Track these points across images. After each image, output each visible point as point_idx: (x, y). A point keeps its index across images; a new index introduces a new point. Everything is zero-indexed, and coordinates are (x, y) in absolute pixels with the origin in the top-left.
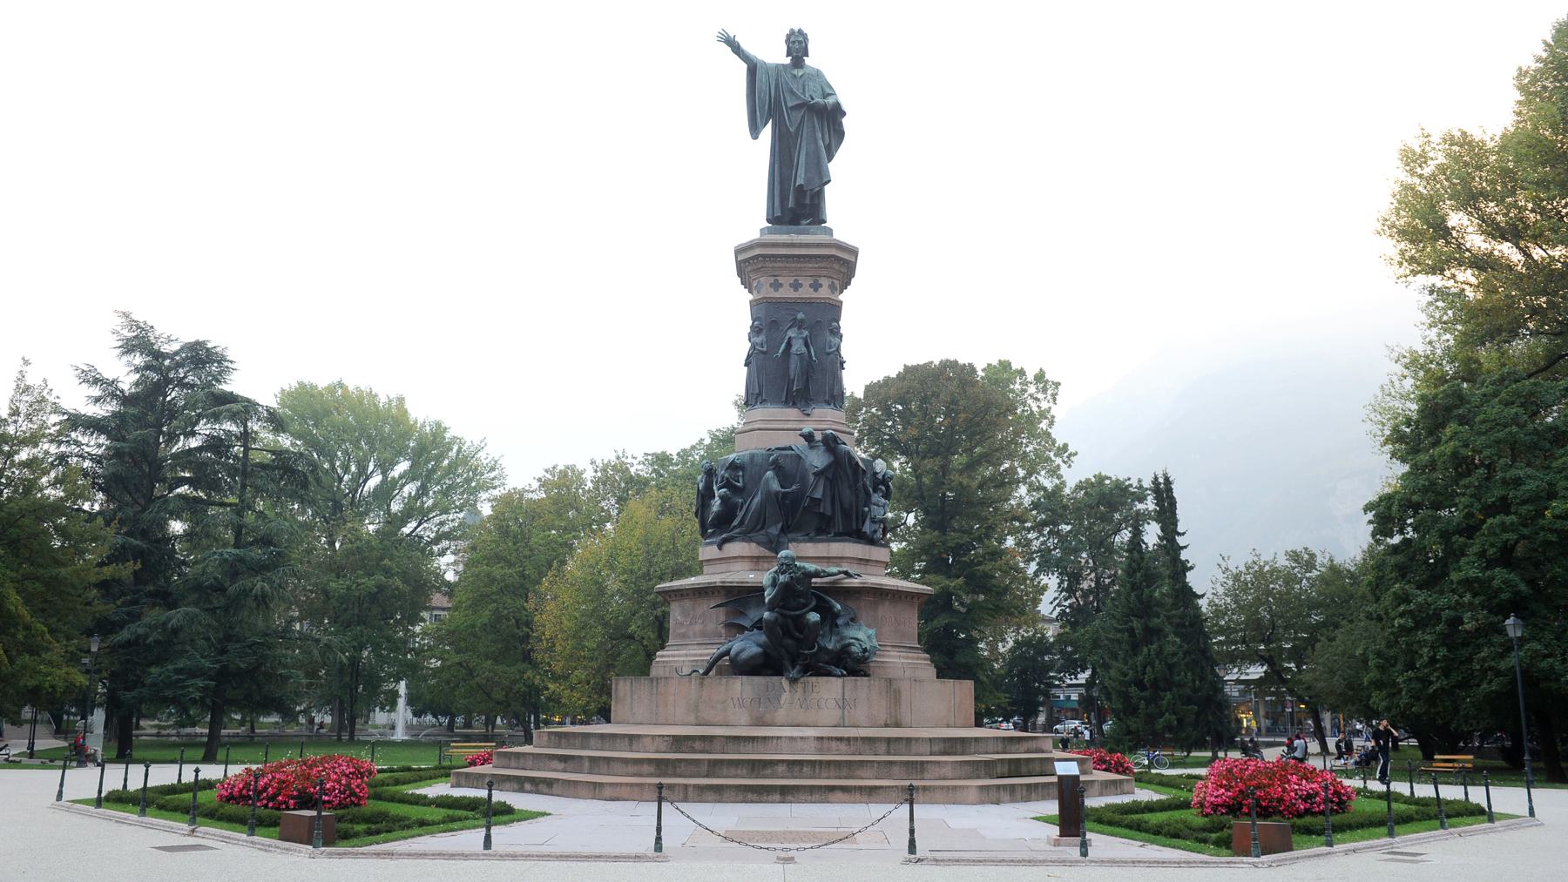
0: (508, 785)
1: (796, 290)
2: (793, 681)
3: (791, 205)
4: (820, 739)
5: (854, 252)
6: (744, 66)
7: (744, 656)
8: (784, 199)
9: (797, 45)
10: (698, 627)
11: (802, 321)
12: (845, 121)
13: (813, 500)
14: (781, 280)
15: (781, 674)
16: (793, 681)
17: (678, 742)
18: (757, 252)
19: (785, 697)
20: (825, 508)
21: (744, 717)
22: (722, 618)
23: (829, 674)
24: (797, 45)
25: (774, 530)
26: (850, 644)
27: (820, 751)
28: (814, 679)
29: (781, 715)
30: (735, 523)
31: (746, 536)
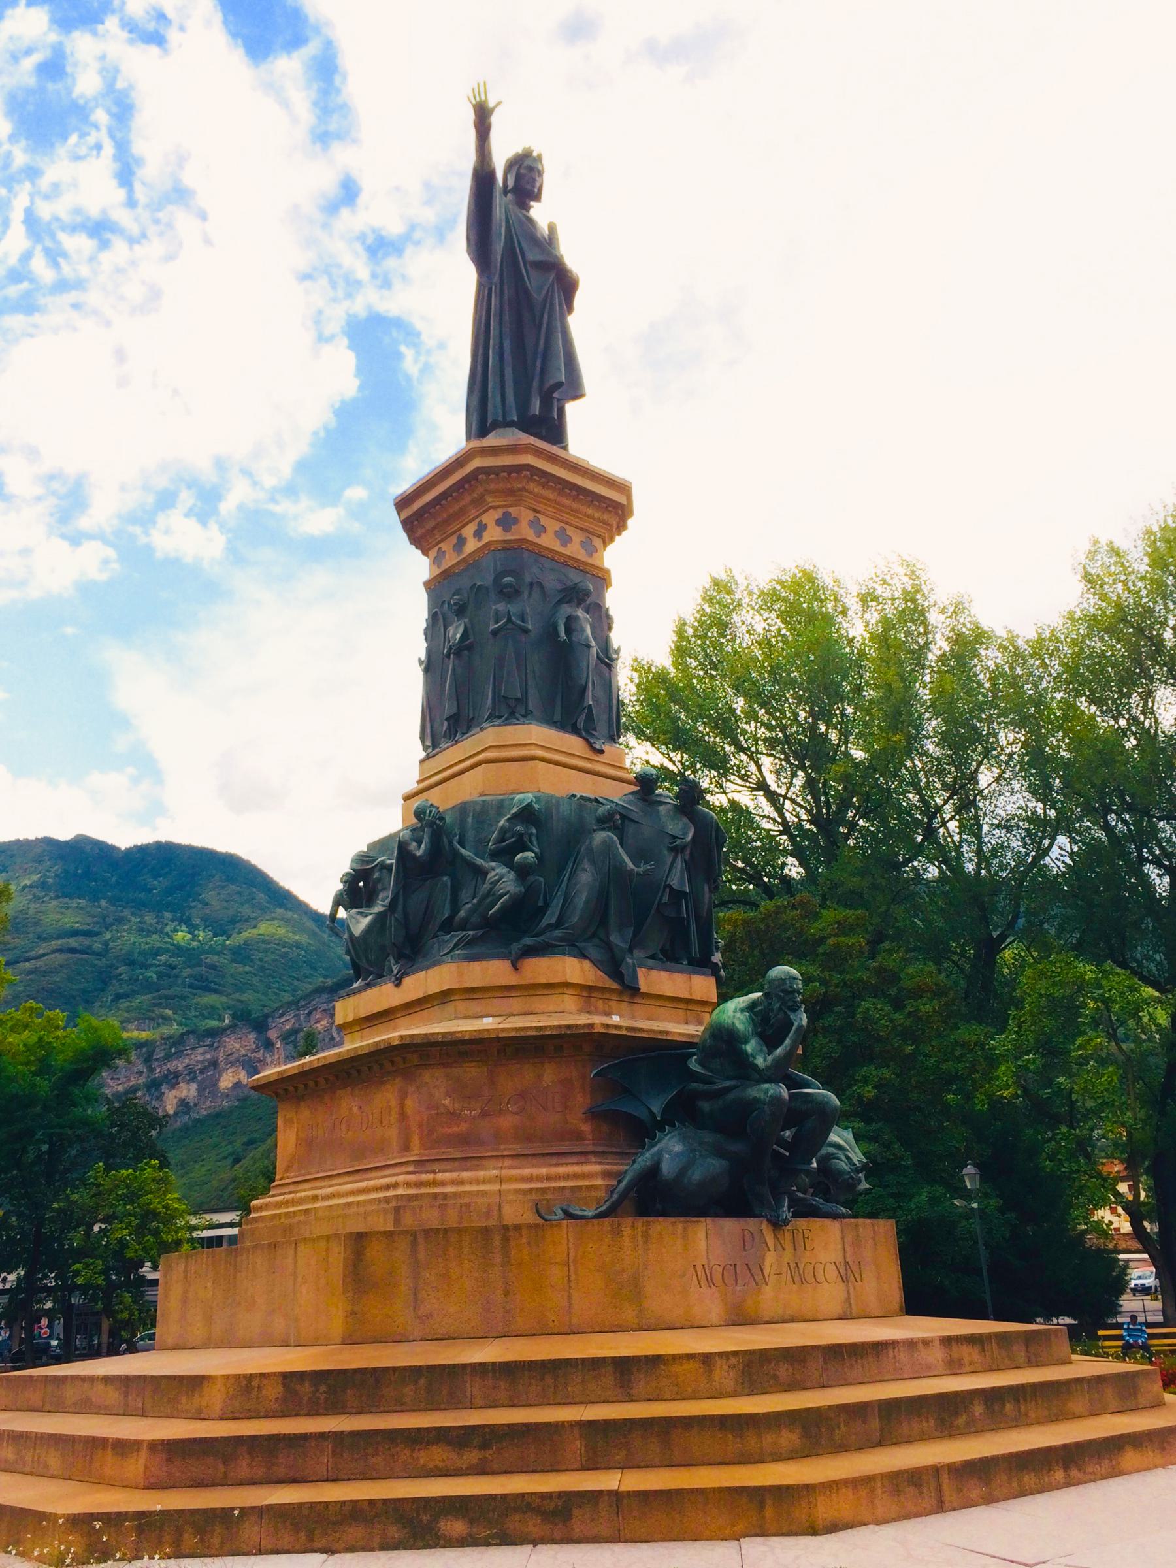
0: (355, 1532)
4: (947, 1341)
10: (507, 1122)
14: (544, 521)
17: (757, 1369)
21: (711, 1305)
22: (581, 1101)
26: (830, 1156)
27: (954, 1367)
29: (769, 1298)
30: (550, 917)
31: (574, 946)
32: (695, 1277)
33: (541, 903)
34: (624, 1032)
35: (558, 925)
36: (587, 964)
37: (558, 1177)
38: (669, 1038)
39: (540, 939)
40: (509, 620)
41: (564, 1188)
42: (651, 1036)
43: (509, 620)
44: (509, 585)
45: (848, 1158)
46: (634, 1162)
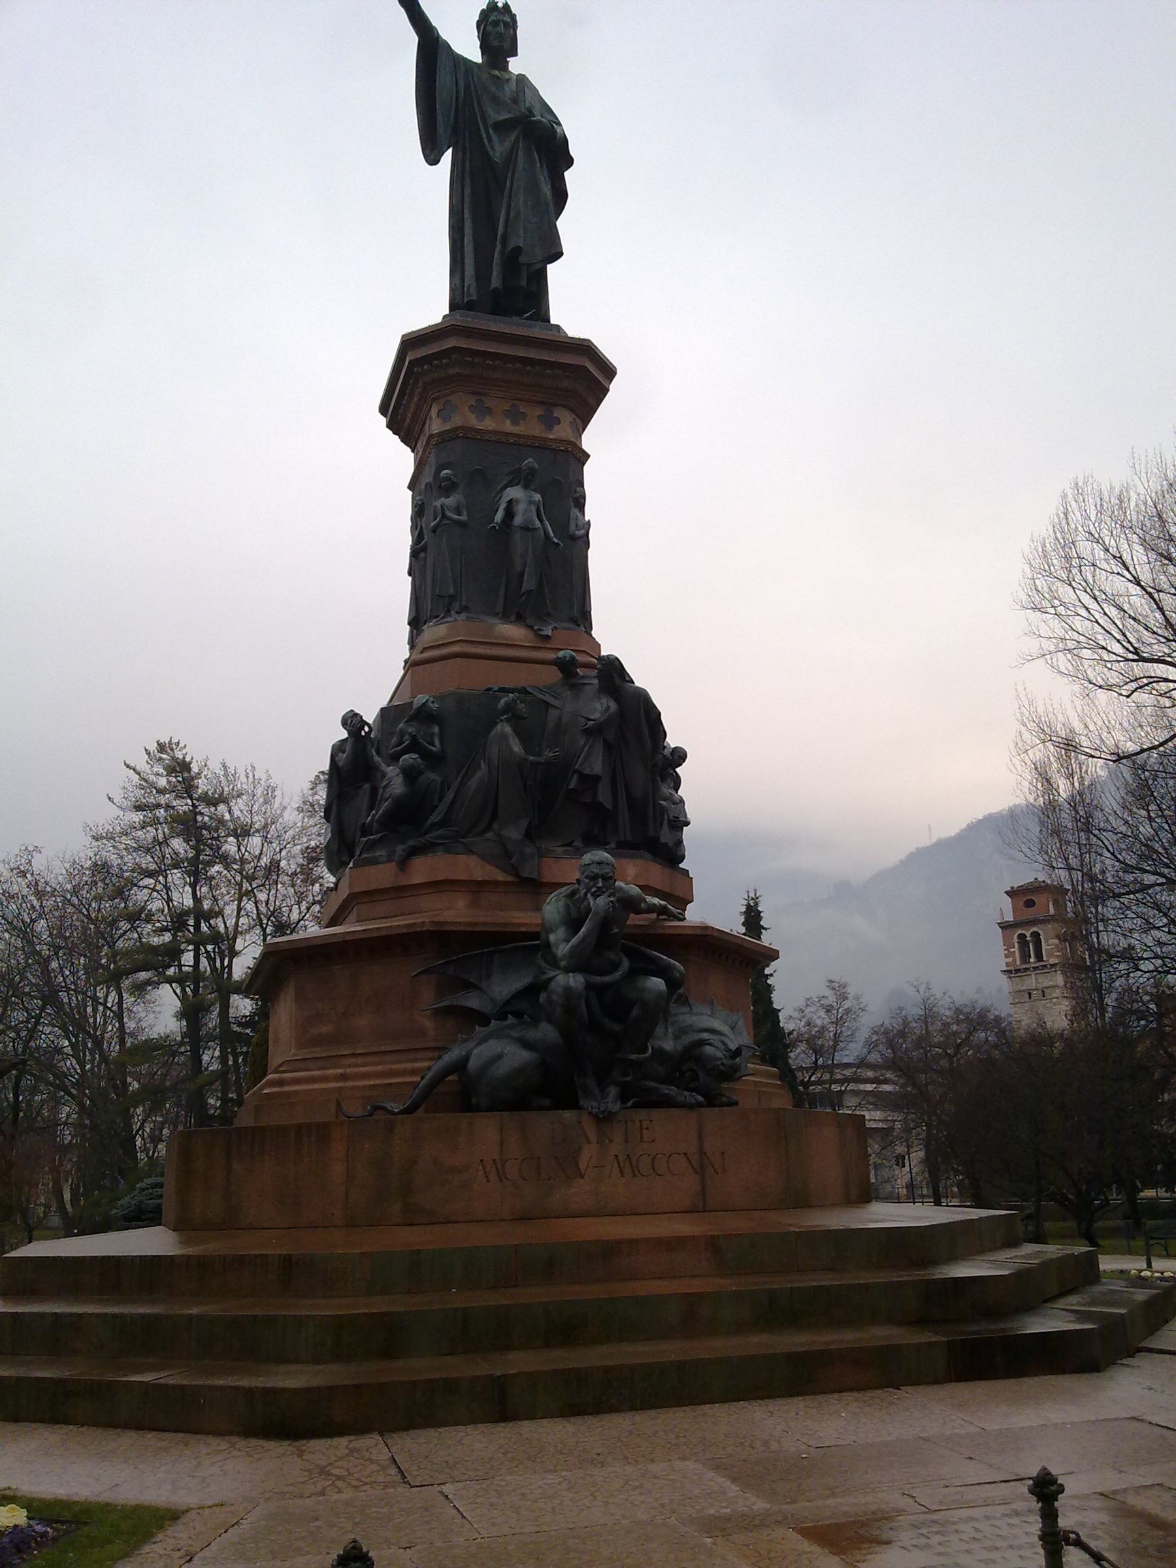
1: (515, 422)
2: (604, 1119)
3: (496, 282)
5: (610, 372)
6: (411, 40)
7: (502, 1069)
8: (482, 276)
9: (498, 30)
11: (532, 472)
12: (568, 174)
13: (583, 777)
15: (574, 1105)
16: (604, 1119)
18: (452, 342)
19: (588, 1155)
20: (604, 795)
23: (667, 1103)
24: (498, 30)
25: (514, 834)
26: (702, 1043)
28: (642, 1114)
30: (435, 817)
32: (481, 1173)
33: (435, 803)
34: (462, 928)
35: (443, 823)
36: (473, 860)
37: (396, 1073)
38: (523, 930)
39: (427, 837)
40: (444, 516)
41: (391, 1084)
42: (497, 929)
43: (444, 516)
44: (447, 478)
45: (724, 1043)
46: (440, 1057)
